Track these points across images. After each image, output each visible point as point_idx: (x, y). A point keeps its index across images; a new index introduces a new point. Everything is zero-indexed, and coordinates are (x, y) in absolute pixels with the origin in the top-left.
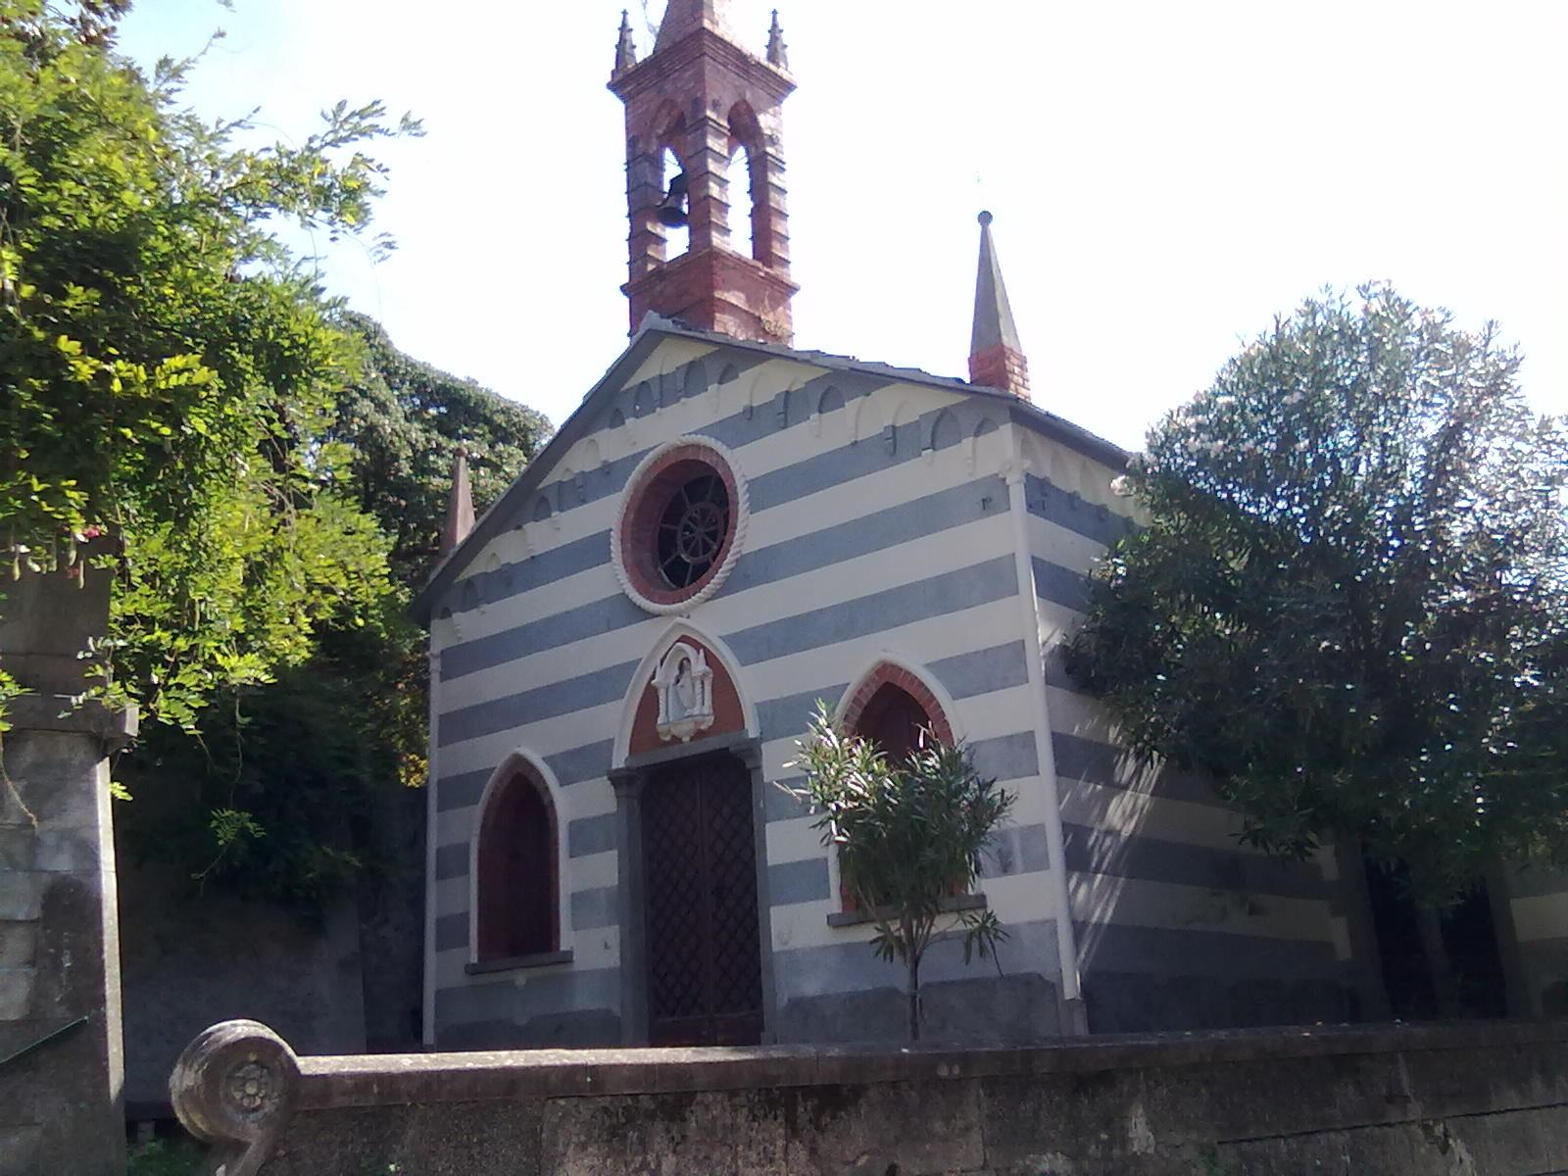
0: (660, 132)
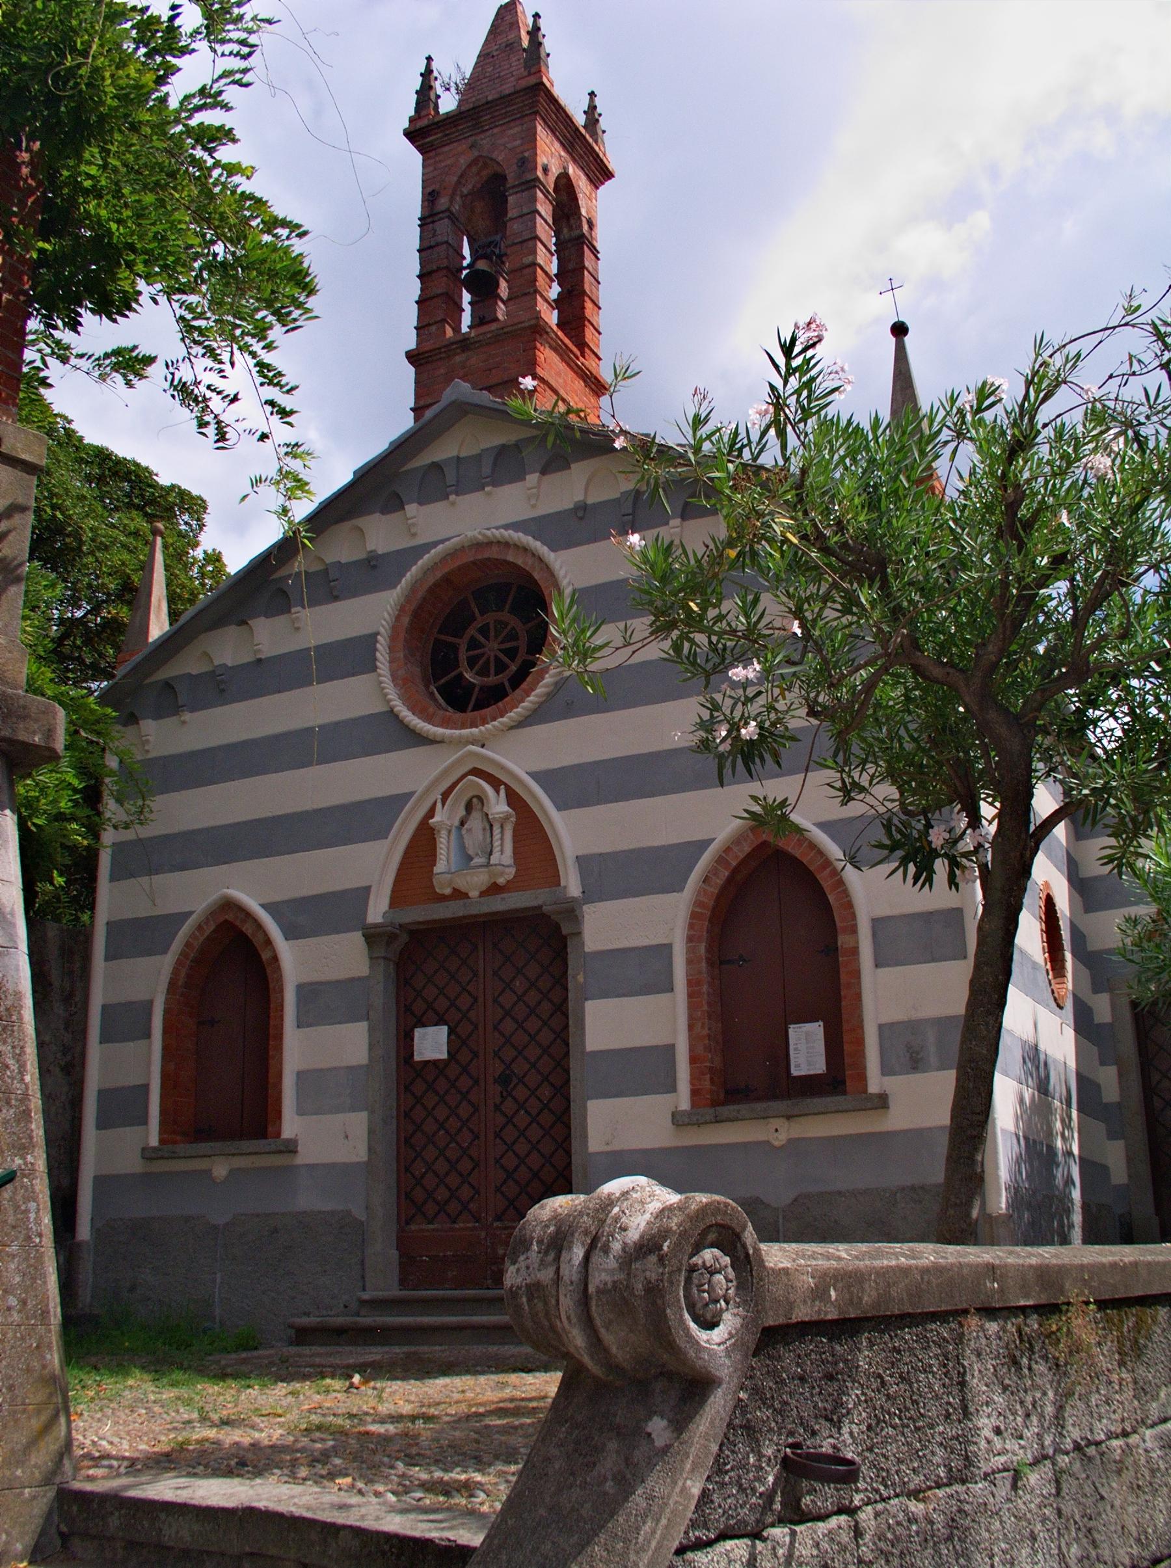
0: (465, 191)
